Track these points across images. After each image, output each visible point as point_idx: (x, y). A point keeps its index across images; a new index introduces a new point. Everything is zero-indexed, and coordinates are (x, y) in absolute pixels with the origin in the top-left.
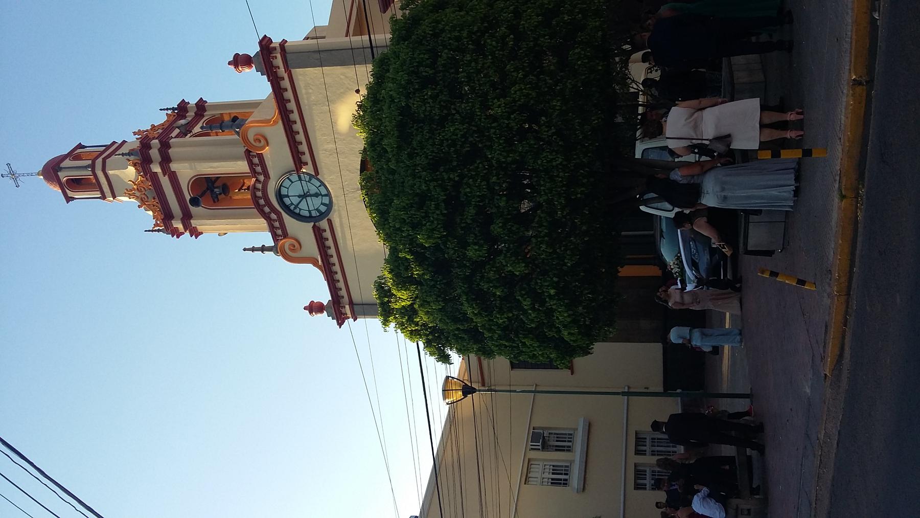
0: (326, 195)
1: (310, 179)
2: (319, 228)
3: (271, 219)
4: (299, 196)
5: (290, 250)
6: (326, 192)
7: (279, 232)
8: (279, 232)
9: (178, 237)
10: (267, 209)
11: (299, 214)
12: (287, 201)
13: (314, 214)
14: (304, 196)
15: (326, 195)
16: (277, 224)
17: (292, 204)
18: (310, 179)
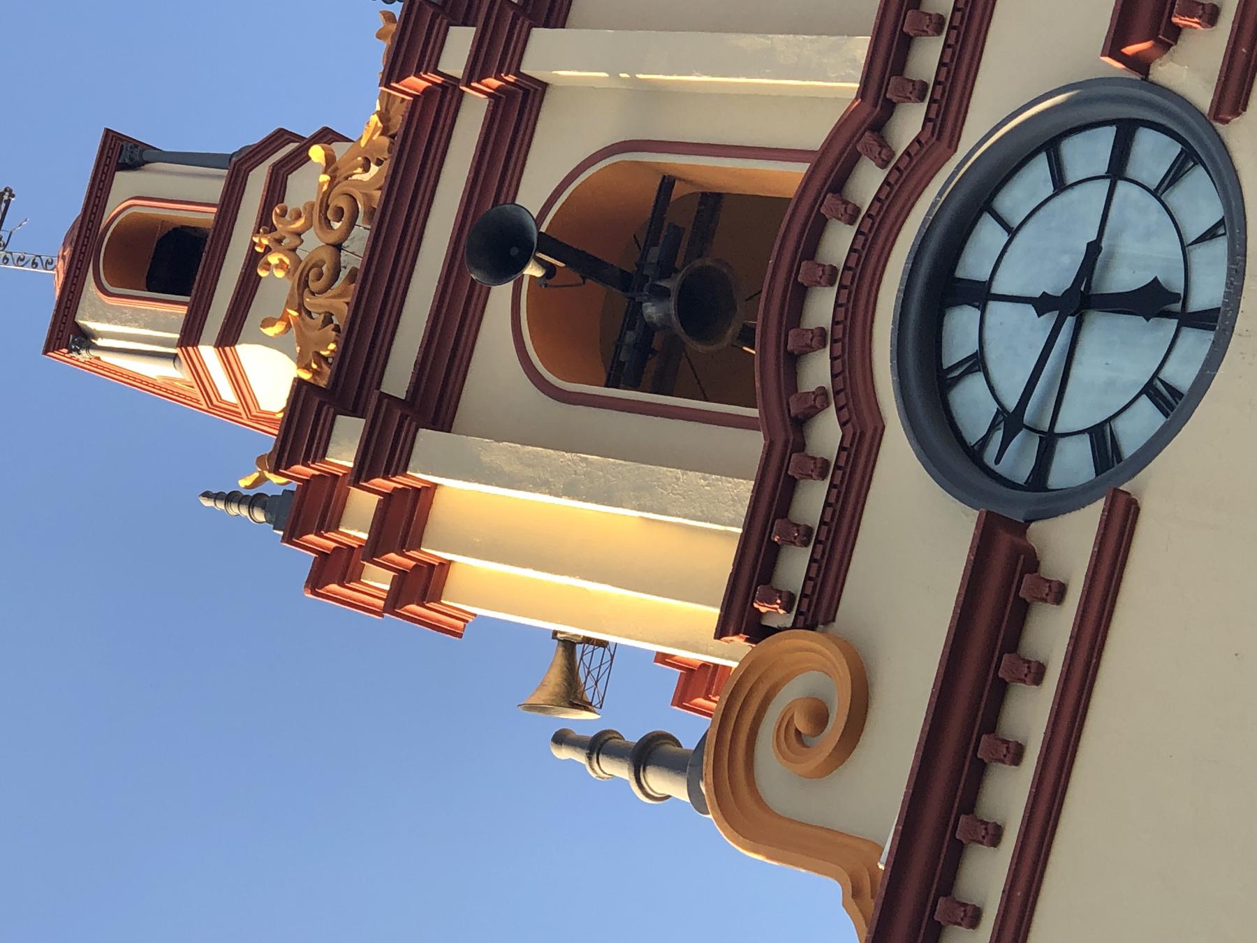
0: (1205, 320)
1: (1174, 175)
2: (1030, 561)
3: (801, 446)
4: (1042, 304)
5: (786, 725)
6: (1207, 292)
7: (795, 567)
8: (795, 567)
9: (316, 582)
10: (818, 371)
11: (974, 454)
12: (961, 328)
13: (1073, 463)
14: (1078, 302)
15: (1205, 320)
16: (811, 501)
17: (977, 363)
18: (1174, 175)
